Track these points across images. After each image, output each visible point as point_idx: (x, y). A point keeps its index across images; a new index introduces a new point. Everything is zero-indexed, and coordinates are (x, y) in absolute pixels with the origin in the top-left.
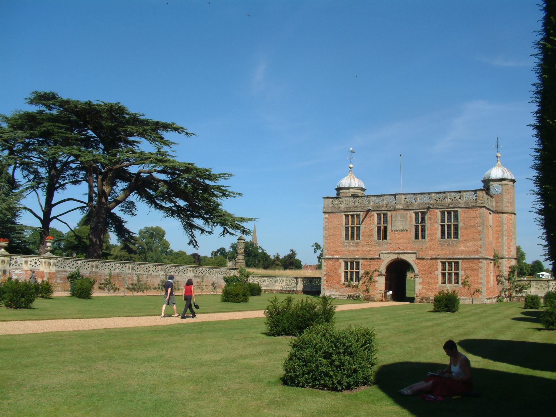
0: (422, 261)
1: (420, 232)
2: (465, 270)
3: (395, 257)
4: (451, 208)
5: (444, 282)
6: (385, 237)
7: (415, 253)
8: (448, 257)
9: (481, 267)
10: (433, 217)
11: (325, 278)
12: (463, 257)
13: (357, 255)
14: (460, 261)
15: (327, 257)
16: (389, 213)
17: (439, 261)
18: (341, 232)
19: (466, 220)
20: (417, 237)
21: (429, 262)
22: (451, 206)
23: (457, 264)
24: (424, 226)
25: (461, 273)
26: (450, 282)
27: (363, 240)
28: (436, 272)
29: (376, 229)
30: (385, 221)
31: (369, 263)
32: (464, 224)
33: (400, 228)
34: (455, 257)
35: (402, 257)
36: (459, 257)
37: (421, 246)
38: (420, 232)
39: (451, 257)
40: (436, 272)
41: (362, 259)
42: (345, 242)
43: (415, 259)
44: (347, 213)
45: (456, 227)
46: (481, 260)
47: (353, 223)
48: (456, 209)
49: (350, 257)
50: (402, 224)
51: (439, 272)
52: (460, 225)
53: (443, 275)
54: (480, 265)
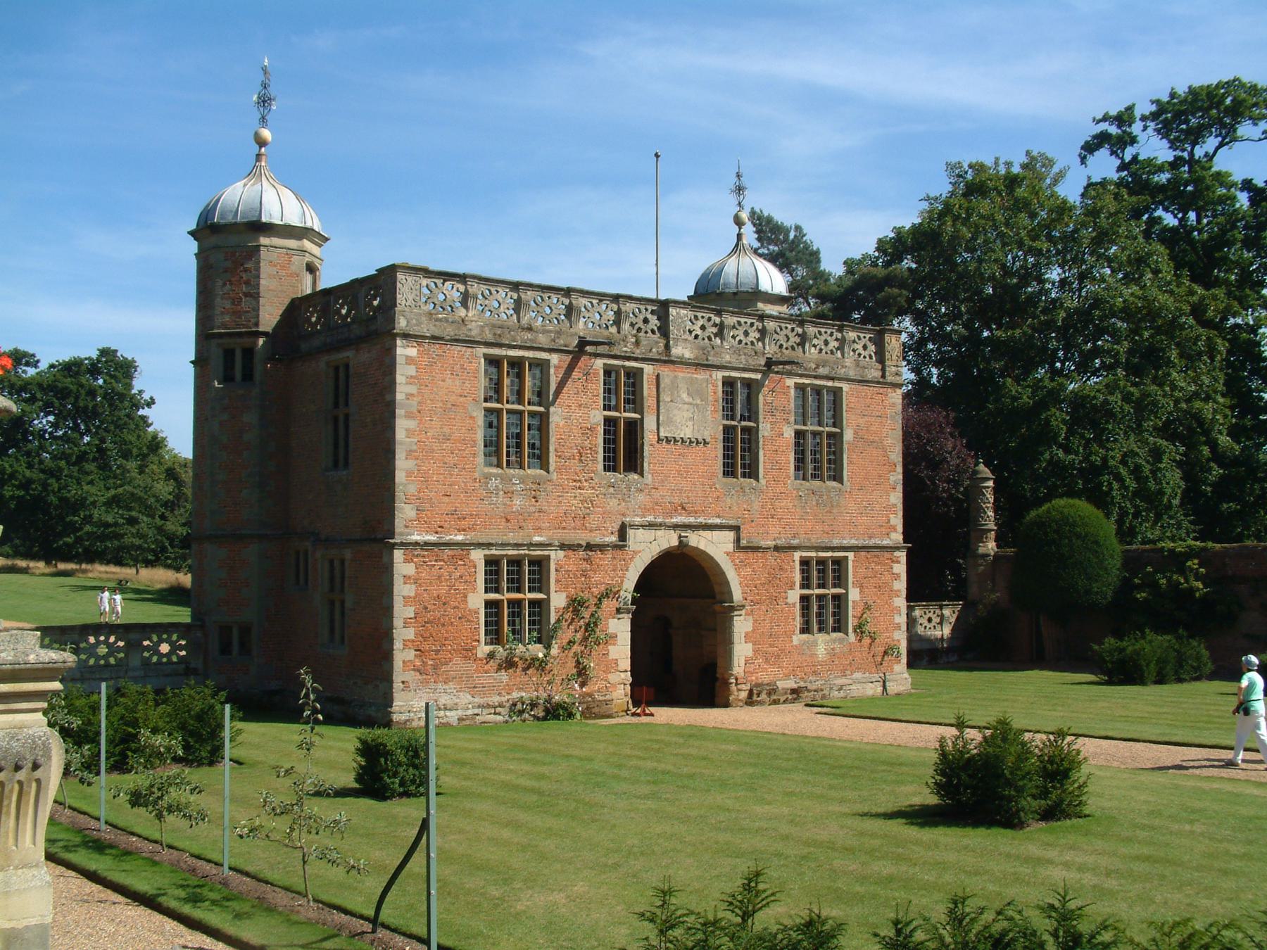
2: (861, 587)
3: (669, 540)
5: (806, 629)
7: (736, 529)
9: (897, 577)
11: (410, 633)
13: (538, 529)
14: (851, 555)
17: (797, 555)
21: (771, 559)
22: (822, 371)
27: (559, 470)
30: (635, 400)
31: (585, 565)
33: (687, 432)
34: (836, 542)
35: (698, 540)
37: (736, 499)
39: (825, 541)
41: (563, 547)
42: (488, 477)
43: (731, 547)
45: (836, 439)
49: (512, 537)
52: (848, 436)
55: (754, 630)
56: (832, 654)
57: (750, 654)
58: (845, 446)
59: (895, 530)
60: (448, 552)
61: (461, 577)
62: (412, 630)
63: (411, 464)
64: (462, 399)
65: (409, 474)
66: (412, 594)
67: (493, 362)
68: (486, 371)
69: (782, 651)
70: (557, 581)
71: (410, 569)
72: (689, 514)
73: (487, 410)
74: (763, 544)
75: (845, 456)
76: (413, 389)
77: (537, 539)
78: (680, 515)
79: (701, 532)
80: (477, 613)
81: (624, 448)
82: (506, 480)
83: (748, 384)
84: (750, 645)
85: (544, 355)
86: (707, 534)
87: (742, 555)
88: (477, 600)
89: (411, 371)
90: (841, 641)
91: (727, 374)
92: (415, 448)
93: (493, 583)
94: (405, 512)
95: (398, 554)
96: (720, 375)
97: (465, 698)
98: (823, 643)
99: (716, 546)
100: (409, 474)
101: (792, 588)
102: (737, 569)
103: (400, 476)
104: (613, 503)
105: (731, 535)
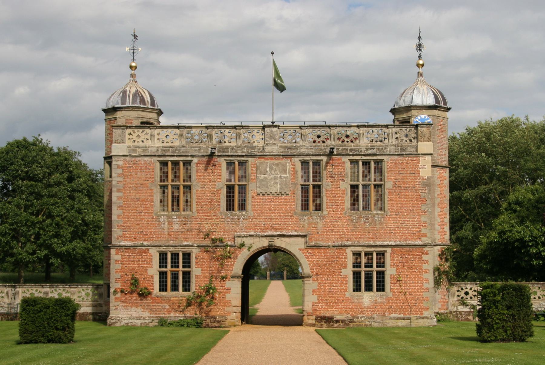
0: (316, 250)
1: (311, 197)
3: (264, 243)
4: (368, 155)
5: (357, 289)
6: (243, 206)
8: (366, 243)
9: (427, 262)
10: (336, 171)
12: (393, 243)
13: (186, 240)
14: (389, 250)
15: (122, 243)
16: (250, 160)
17: (349, 251)
18: (151, 195)
19: (399, 177)
20: (305, 207)
21: (330, 252)
22: (370, 152)
23: (381, 254)
24: (319, 187)
25: (390, 271)
26: (369, 288)
27: (198, 211)
28: (344, 272)
29: (225, 190)
30: (244, 177)
32: (395, 184)
34: (378, 243)
35: (279, 243)
36: (386, 243)
37: (312, 221)
38: (311, 197)
39: (371, 243)
40: (343, 270)
41: (199, 247)
42: (161, 216)
43: (303, 246)
44: (162, 159)
46: (426, 249)
47: (176, 176)
48: (379, 158)
49: (171, 243)
50: (275, 180)
51: (349, 272)
52: (388, 185)
53: (357, 276)
54: (425, 257)
55: (318, 289)
56: (375, 303)
57: (316, 301)
58: (386, 191)
59: (426, 236)
60: (137, 249)
61: (145, 261)
62: (119, 284)
63: (120, 212)
64: (145, 182)
65: (119, 216)
66: (120, 268)
67: (164, 164)
68: (161, 169)
69: (338, 300)
70: (197, 263)
71: (119, 257)
72: (276, 230)
73: (161, 186)
74: (324, 244)
75: (386, 197)
76: (121, 179)
77: (185, 243)
78: (271, 230)
79: (283, 239)
80: (152, 276)
81: (235, 199)
82: (170, 217)
83: (317, 163)
84: (315, 297)
85: (189, 158)
86: (287, 240)
87: (310, 250)
88: (154, 271)
89: (120, 171)
90: (381, 296)
91: (302, 158)
92: (122, 205)
93: (163, 262)
94: (116, 232)
95: (113, 251)
96: (297, 159)
97: (147, 314)
98: (367, 298)
99: (295, 247)
100: (119, 216)
101: (345, 267)
102: (308, 259)
103: (114, 217)
104: (228, 227)
105: (303, 240)
